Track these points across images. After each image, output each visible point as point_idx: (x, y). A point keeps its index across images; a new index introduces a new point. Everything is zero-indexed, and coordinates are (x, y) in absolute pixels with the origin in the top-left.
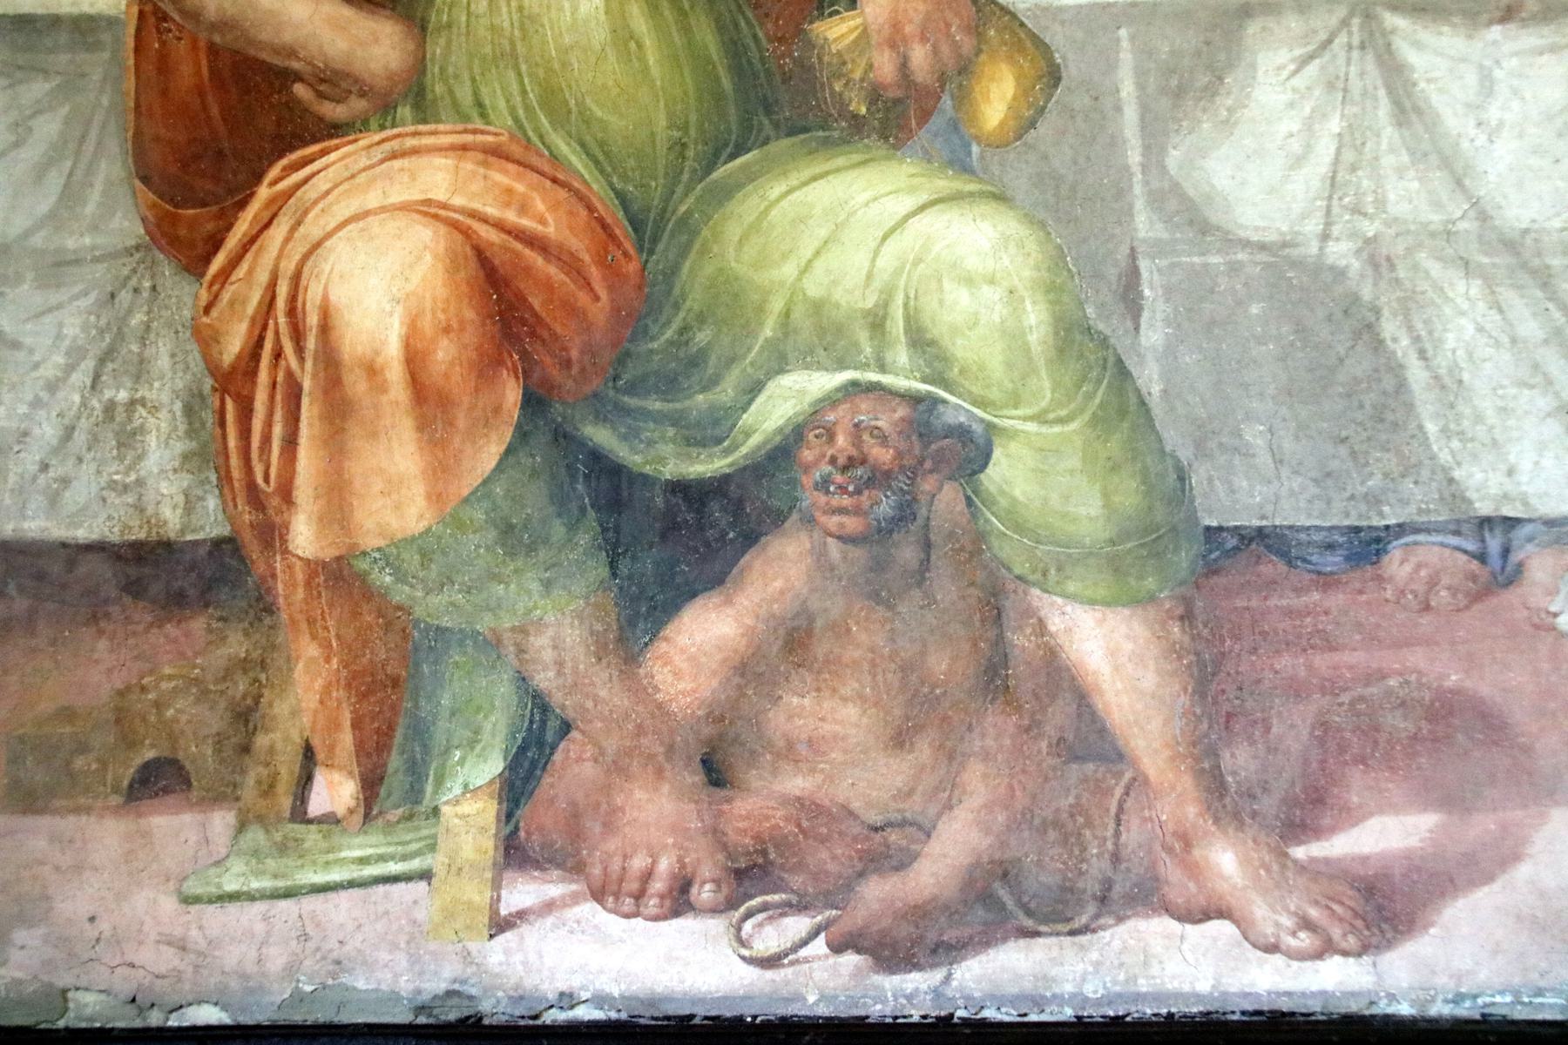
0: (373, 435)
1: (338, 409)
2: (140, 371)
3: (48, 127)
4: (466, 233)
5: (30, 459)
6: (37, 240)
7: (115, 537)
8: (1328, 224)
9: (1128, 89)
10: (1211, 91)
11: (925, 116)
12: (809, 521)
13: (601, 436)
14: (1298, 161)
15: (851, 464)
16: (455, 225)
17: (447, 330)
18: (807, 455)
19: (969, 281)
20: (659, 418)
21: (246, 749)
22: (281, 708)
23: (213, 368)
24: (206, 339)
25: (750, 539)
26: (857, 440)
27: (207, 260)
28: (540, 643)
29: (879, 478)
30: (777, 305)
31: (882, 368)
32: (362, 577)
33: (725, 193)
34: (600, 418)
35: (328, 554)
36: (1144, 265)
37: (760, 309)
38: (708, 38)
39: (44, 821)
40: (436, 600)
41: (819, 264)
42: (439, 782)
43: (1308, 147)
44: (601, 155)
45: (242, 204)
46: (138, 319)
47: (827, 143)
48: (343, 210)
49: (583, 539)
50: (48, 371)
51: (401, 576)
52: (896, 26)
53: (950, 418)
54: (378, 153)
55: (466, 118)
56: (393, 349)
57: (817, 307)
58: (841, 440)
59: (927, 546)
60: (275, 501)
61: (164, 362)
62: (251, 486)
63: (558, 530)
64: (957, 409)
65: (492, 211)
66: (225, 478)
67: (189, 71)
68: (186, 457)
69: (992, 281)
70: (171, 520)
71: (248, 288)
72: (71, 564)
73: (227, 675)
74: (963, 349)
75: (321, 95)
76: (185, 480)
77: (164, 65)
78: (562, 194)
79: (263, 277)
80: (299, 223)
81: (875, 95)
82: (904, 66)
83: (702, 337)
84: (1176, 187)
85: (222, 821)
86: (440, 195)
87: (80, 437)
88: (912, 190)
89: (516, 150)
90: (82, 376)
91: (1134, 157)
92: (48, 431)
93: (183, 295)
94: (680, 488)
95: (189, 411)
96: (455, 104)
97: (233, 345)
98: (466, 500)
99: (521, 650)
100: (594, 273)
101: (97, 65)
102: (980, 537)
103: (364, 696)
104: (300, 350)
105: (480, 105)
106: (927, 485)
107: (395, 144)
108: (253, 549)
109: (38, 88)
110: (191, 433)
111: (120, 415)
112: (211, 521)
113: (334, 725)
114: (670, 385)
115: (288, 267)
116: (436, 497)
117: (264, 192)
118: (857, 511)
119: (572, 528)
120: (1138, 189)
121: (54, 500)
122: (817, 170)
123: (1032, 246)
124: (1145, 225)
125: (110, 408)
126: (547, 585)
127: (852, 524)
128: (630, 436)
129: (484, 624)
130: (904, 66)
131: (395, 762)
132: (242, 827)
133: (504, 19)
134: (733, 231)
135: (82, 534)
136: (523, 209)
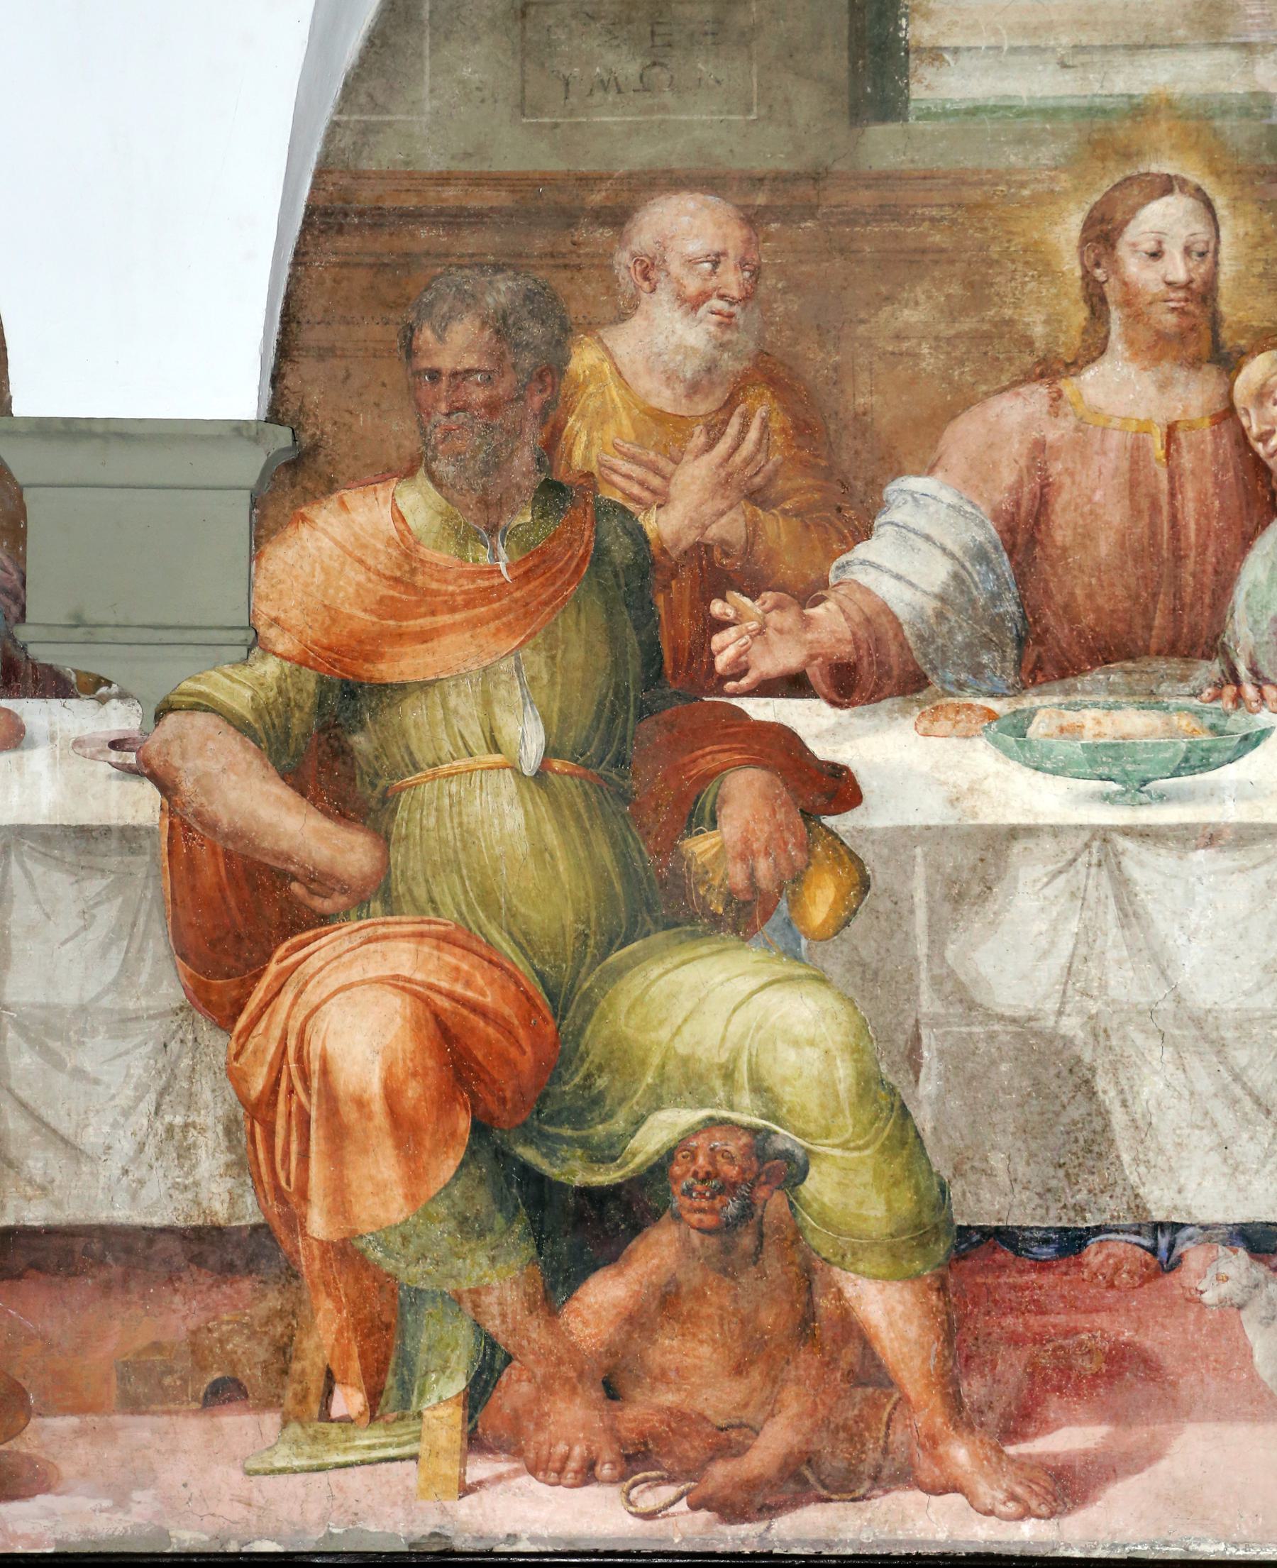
0: (365, 1151)
1: (338, 1134)
2: (190, 1101)
3: (107, 915)
4: (426, 1002)
5: (114, 1166)
6: (106, 1002)
7: (181, 1223)
8: (1063, 1003)
9: (920, 896)
10: (983, 898)
11: (766, 916)
12: (677, 1217)
13: (529, 1154)
14: (1045, 955)
15: (708, 1177)
16: (416, 995)
17: (415, 1074)
18: (677, 1170)
19: (796, 1043)
20: (570, 1142)
21: (285, 1372)
22: (309, 1344)
23: (243, 1100)
24: (237, 1079)
25: (636, 1229)
26: (713, 1162)
27: (234, 1020)
28: (489, 1300)
29: (727, 1188)
30: (655, 1060)
31: (731, 1107)
32: (361, 1253)
33: (618, 972)
34: (528, 1142)
35: (336, 1237)
36: (924, 1032)
37: (643, 1063)
38: (605, 854)
39: (147, 1419)
40: (415, 1270)
41: (686, 1030)
42: (422, 1394)
43: (1053, 943)
44: (525, 944)
45: (258, 977)
46: (186, 1062)
47: (694, 936)
48: (334, 982)
49: (518, 1228)
50: (122, 1101)
51: (388, 1253)
52: (746, 842)
53: (780, 1145)
54: (357, 938)
55: (423, 912)
56: (375, 1088)
57: (685, 1061)
58: (701, 1160)
59: (761, 1235)
60: (295, 1199)
61: (207, 1096)
62: (277, 1187)
63: (499, 1222)
64: (785, 1139)
65: (445, 985)
66: (258, 1181)
67: (210, 872)
68: (228, 1166)
69: (812, 1043)
70: (220, 1212)
71: (266, 1040)
72: (150, 1242)
73: (268, 1321)
74: (788, 1094)
75: (312, 893)
76: (229, 1183)
77: (192, 866)
78: (497, 973)
79: (276, 1033)
80: (301, 992)
81: (730, 897)
82: (752, 876)
83: (601, 1082)
84: (951, 974)
85: (271, 1420)
86: (406, 972)
87: (150, 1150)
88: (756, 973)
89: (461, 937)
90: (147, 1105)
91: (922, 949)
92: (126, 1146)
93: (218, 1045)
94: (586, 1192)
95: (228, 1132)
96: (414, 900)
97: (258, 1084)
98: (433, 1200)
99: (476, 1306)
100: (521, 1033)
101: (141, 865)
102: (798, 1231)
103: (366, 1337)
104: (307, 1089)
105: (432, 900)
106: (761, 1193)
107: (369, 932)
108: (282, 1233)
109: (96, 885)
110: (231, 1149)
111: (178, 1135)
112: (250, 1213)
113: (347, 1356)
114: (578, 1118)
115: (295, 1025)
116: (411, 1198)
117: (273, 968)
118: (712, 1211)
119: (510, 1221)
120: (924, 975)
121: (134, 1196)
122: (686, 955)
123: (843, 1017)
124: (928, 1003)
125: (170, 1129)
126: (493, 1260)
127: (708, 1220)
128: (550, 1154)
129: (449, 1287)
130: (752, 876)
131: (390, 1381)
132: (285, 1425)
133: (449, 833)
134: (624, 1003)
135: (157, 1221)
136: (468, 984)
